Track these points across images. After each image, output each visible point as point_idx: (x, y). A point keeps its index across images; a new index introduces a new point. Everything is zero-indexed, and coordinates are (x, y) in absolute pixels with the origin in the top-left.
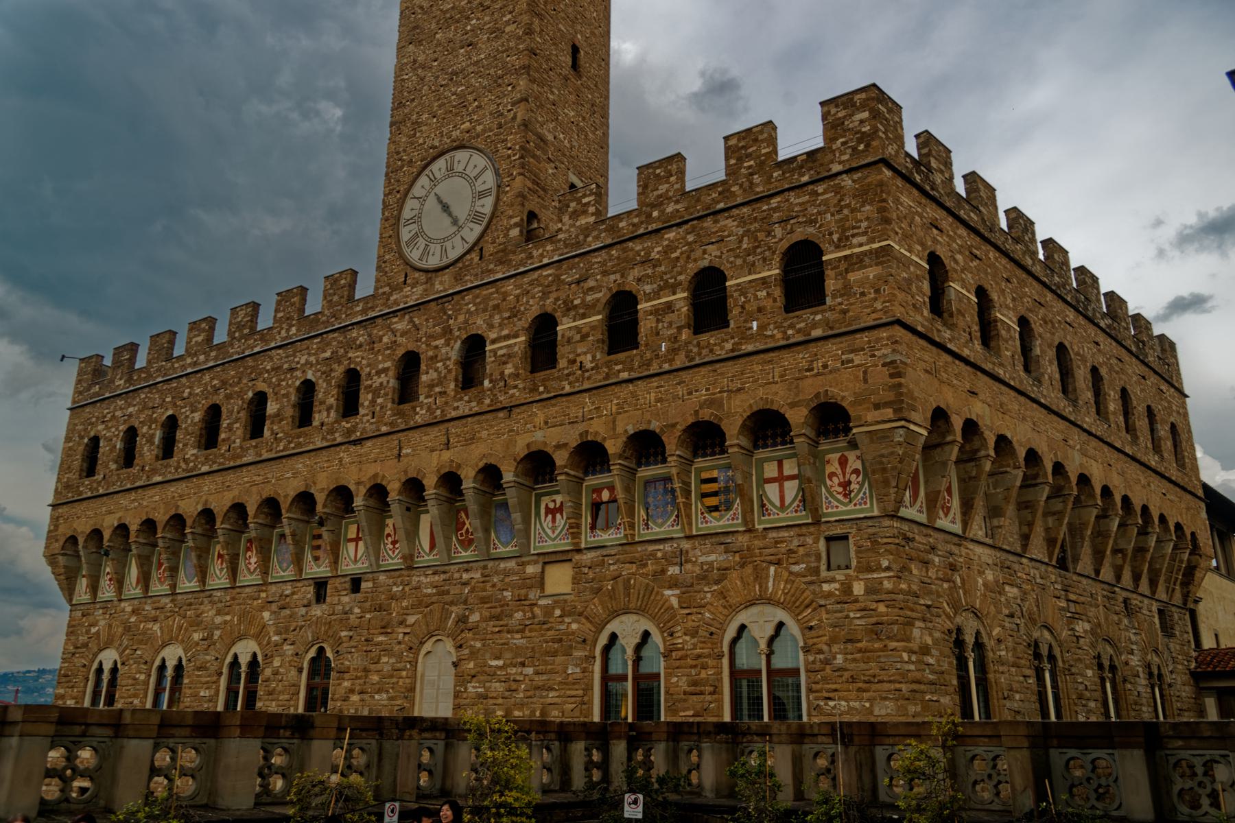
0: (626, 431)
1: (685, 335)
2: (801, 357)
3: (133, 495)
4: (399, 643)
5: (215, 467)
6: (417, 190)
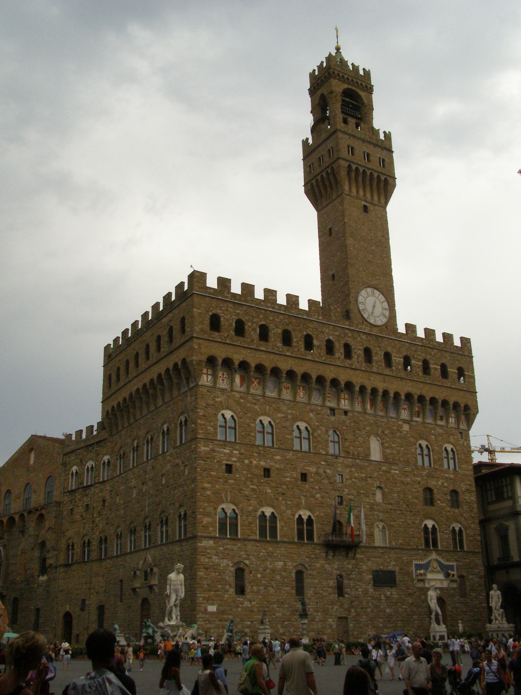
1: (441, 378)
2: (462, 393)
3: (249, 351)
5: (293, 355)
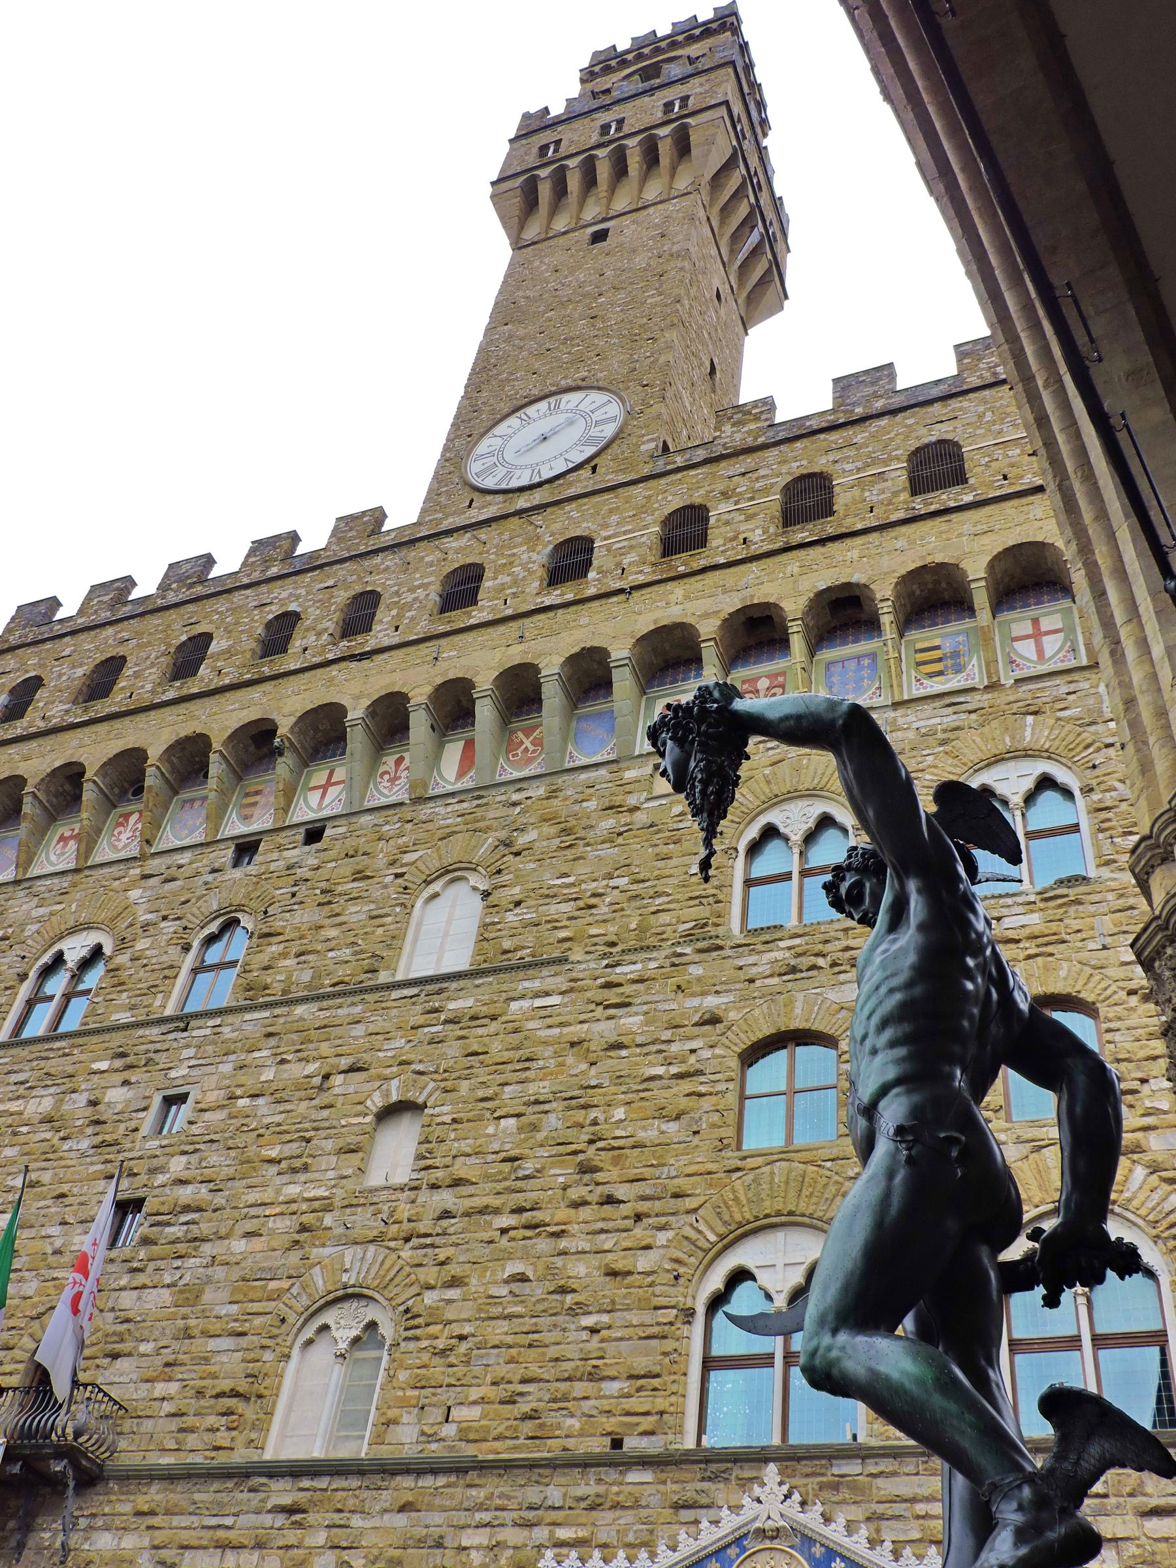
0: (815, 587)
1: (904, 496)
4: (386, 887)
6: (501, 429)
